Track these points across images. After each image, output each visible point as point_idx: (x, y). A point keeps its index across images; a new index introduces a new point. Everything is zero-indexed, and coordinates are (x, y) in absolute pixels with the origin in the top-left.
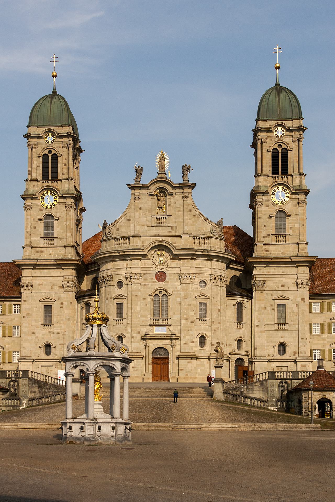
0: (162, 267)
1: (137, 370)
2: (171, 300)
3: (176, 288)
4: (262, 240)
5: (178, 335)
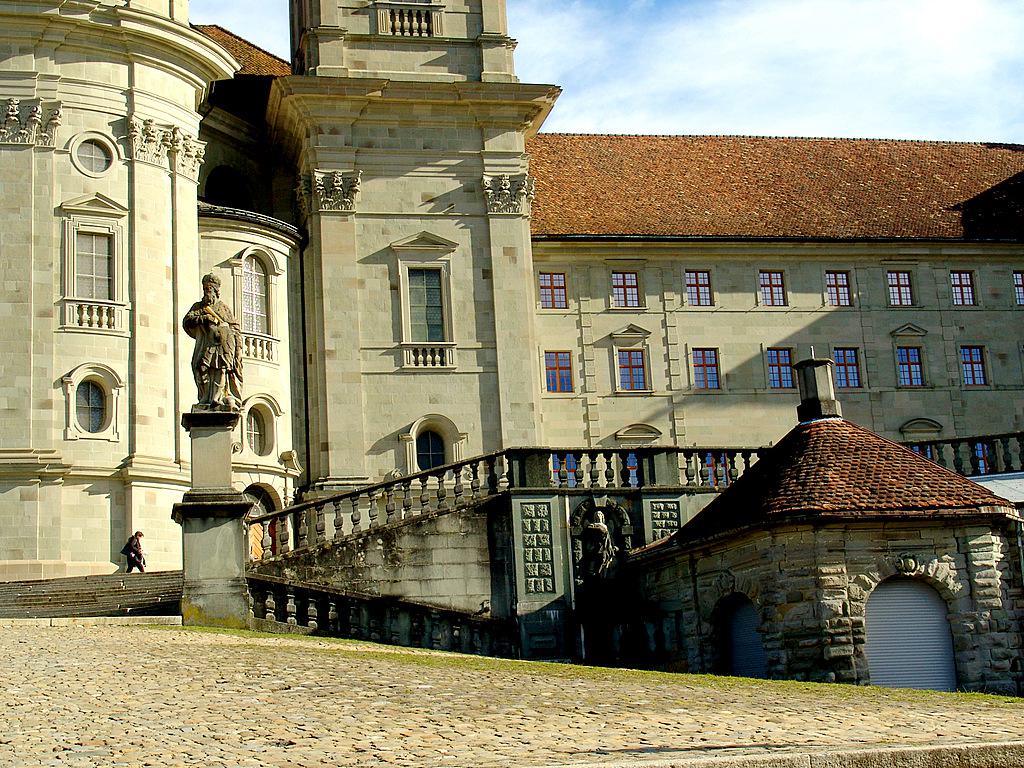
4: (340, 21)
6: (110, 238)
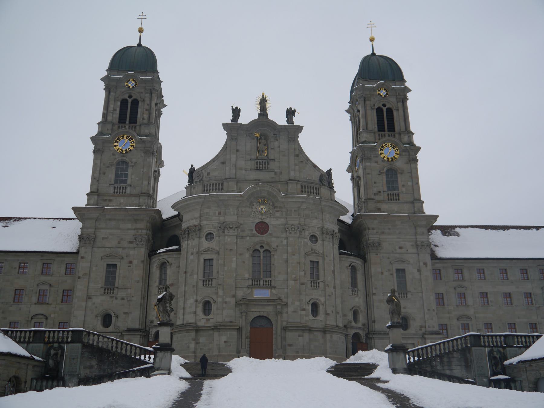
0: (264, 217)
1: (230, 345)
2: (276, 257)
3: (282, 242)
4: (372, 197)
5: (285, 300)
6: (318, 262)
